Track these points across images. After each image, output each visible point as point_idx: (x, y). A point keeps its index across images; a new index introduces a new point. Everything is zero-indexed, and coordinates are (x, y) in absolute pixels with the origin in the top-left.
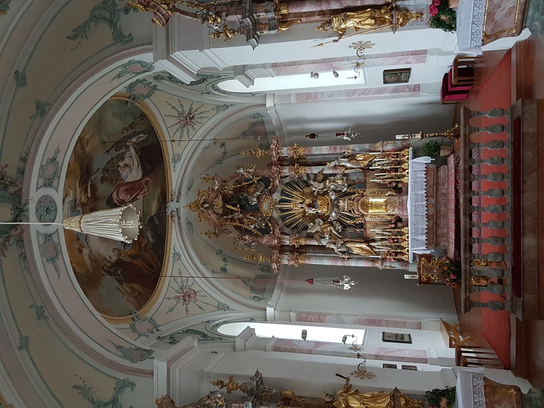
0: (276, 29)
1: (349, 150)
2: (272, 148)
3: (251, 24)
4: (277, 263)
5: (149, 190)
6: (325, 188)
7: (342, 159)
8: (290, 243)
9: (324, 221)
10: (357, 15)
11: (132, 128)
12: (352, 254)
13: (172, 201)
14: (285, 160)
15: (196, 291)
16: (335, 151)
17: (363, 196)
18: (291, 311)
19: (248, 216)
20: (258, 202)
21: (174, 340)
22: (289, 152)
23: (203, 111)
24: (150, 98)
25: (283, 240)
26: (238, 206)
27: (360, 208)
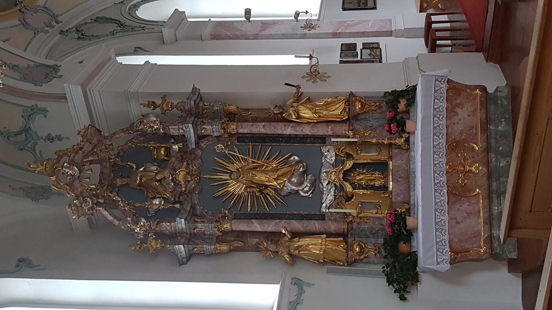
21: (82, 35)
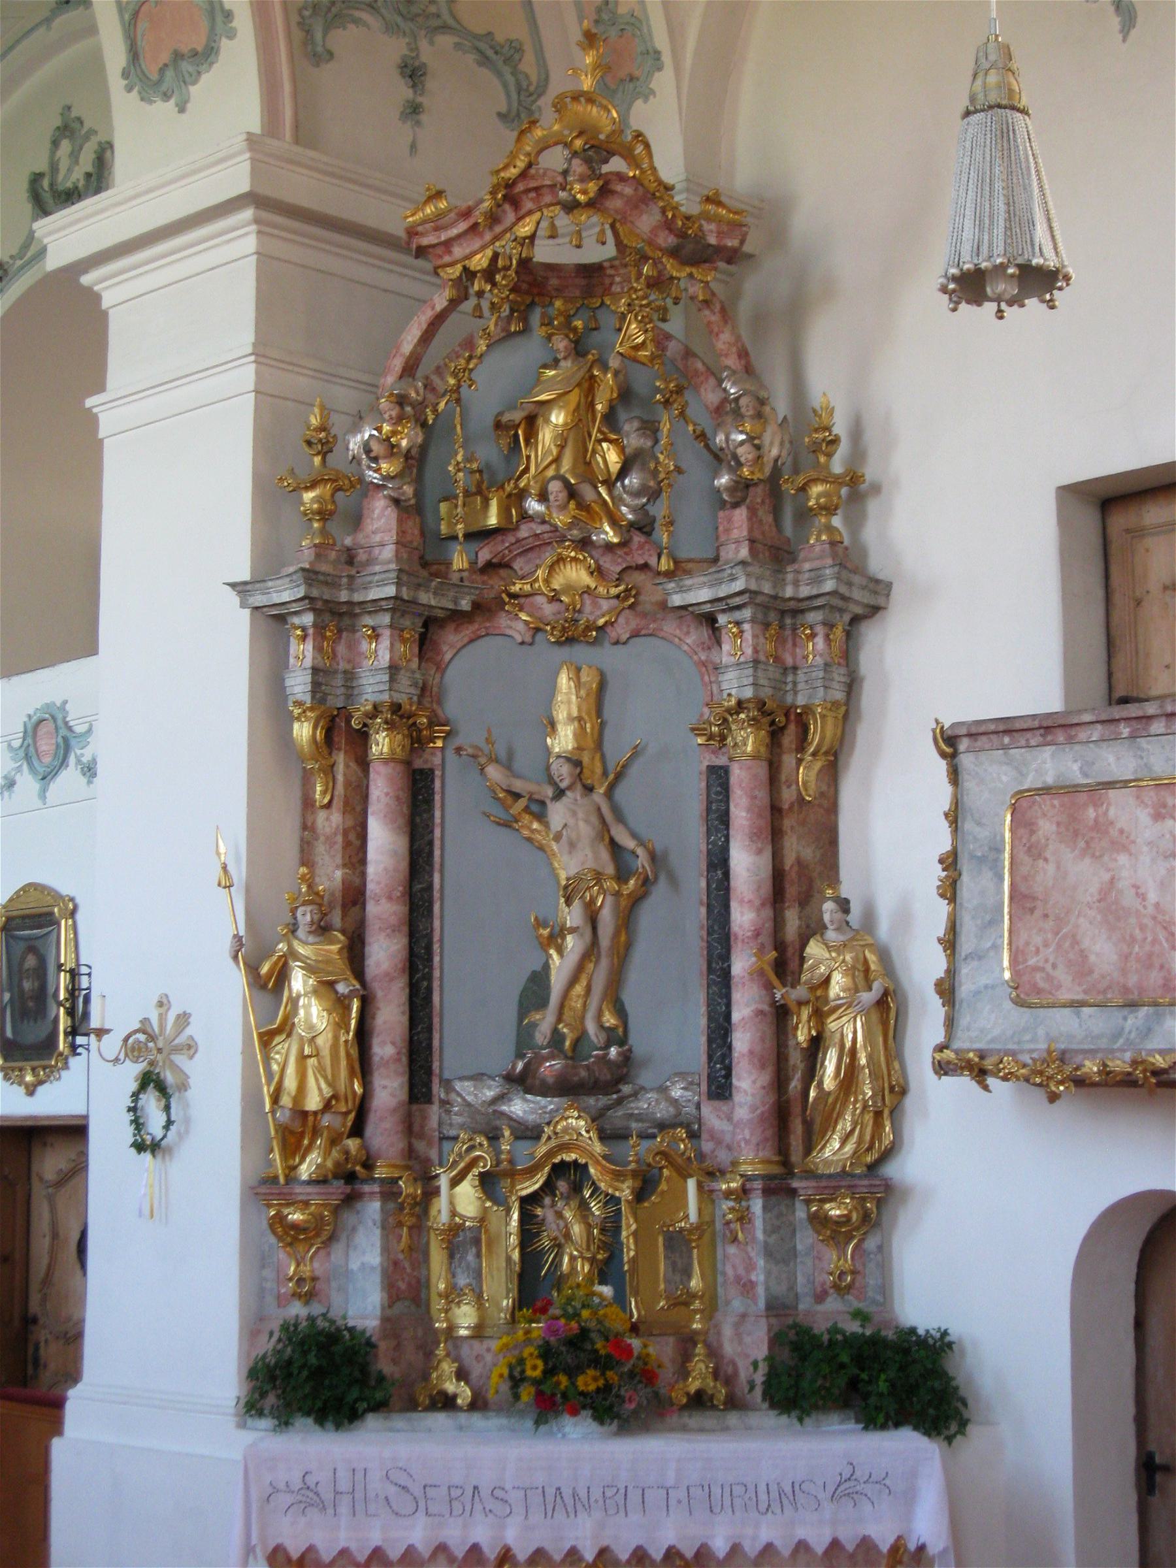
0: (313, 698)
3: (357, 597)
10: (346, 1042)
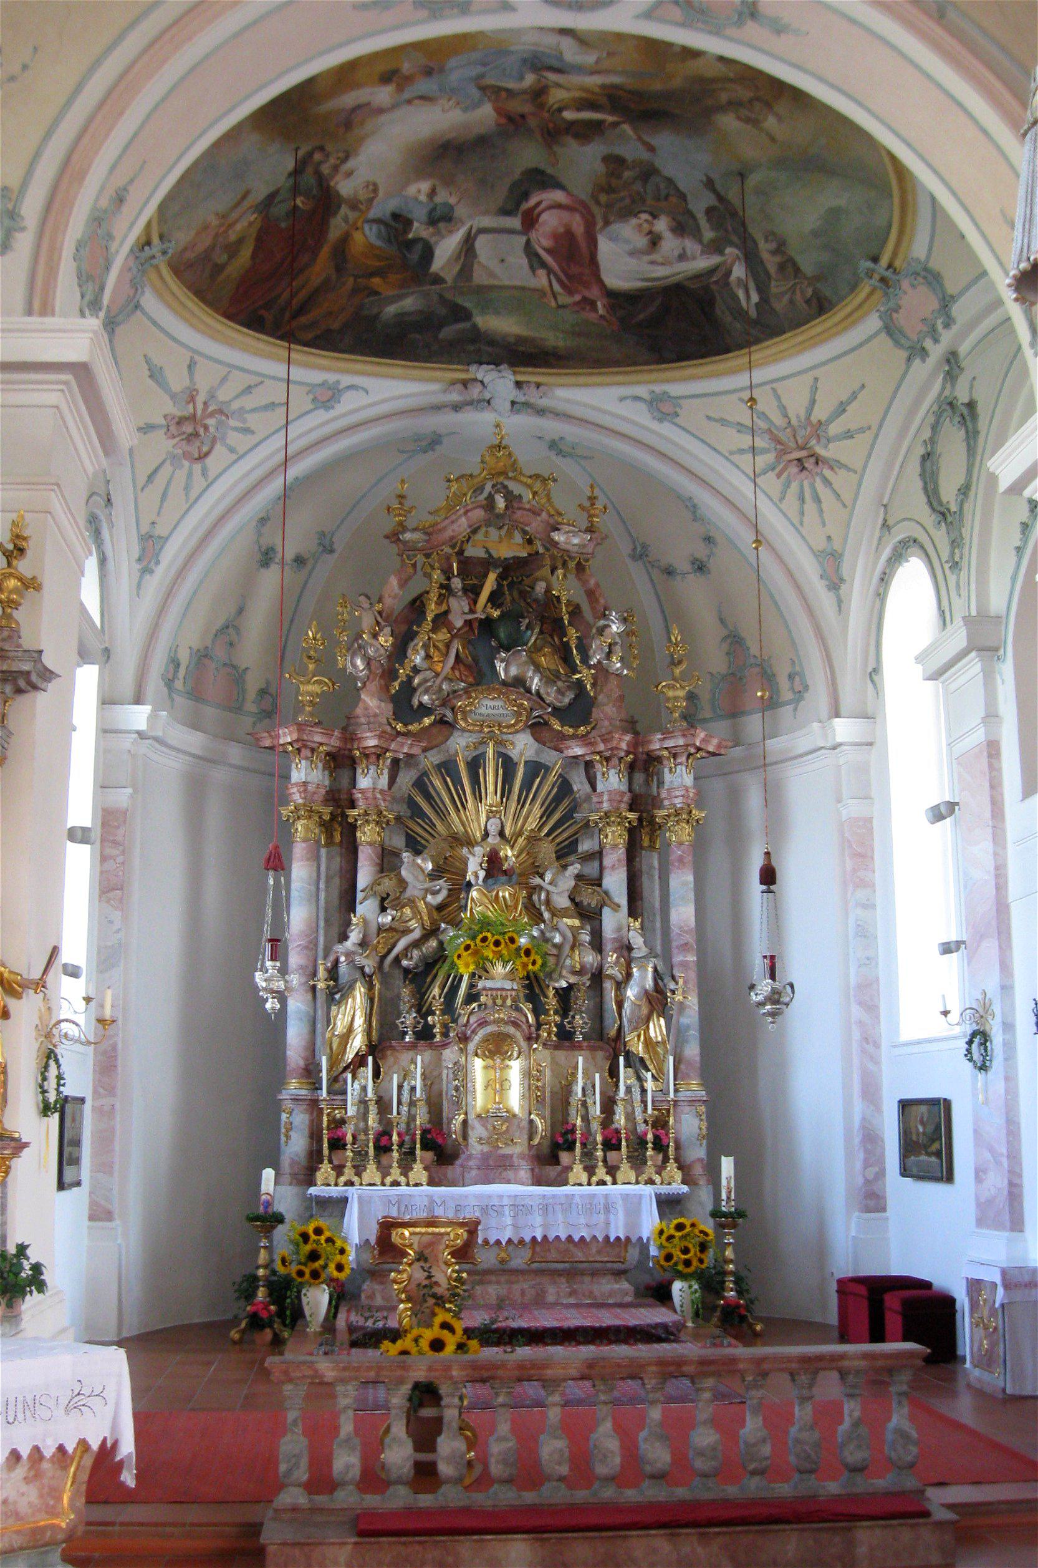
1: (684, 992)
2: (693, 735)
4: (296, 746)
5: (561, 311)
6: (553, 915)
7: (650, 970)
8: (363, 791)
9: (440, 908)
11: (782, 267)
12: (331, 999)
13: (518, 384)
14: (649, 776)
15: (209, 461)
16: (677, 947)
17: (529, 1039)
18: (135, 790)
19: (457, 645)
20: (504, 683)
22: (677, 793)
23: (824, 505)
24: (883, 335)
25: (372, 768)
26: (496, 614)
27: (489, 1029)
